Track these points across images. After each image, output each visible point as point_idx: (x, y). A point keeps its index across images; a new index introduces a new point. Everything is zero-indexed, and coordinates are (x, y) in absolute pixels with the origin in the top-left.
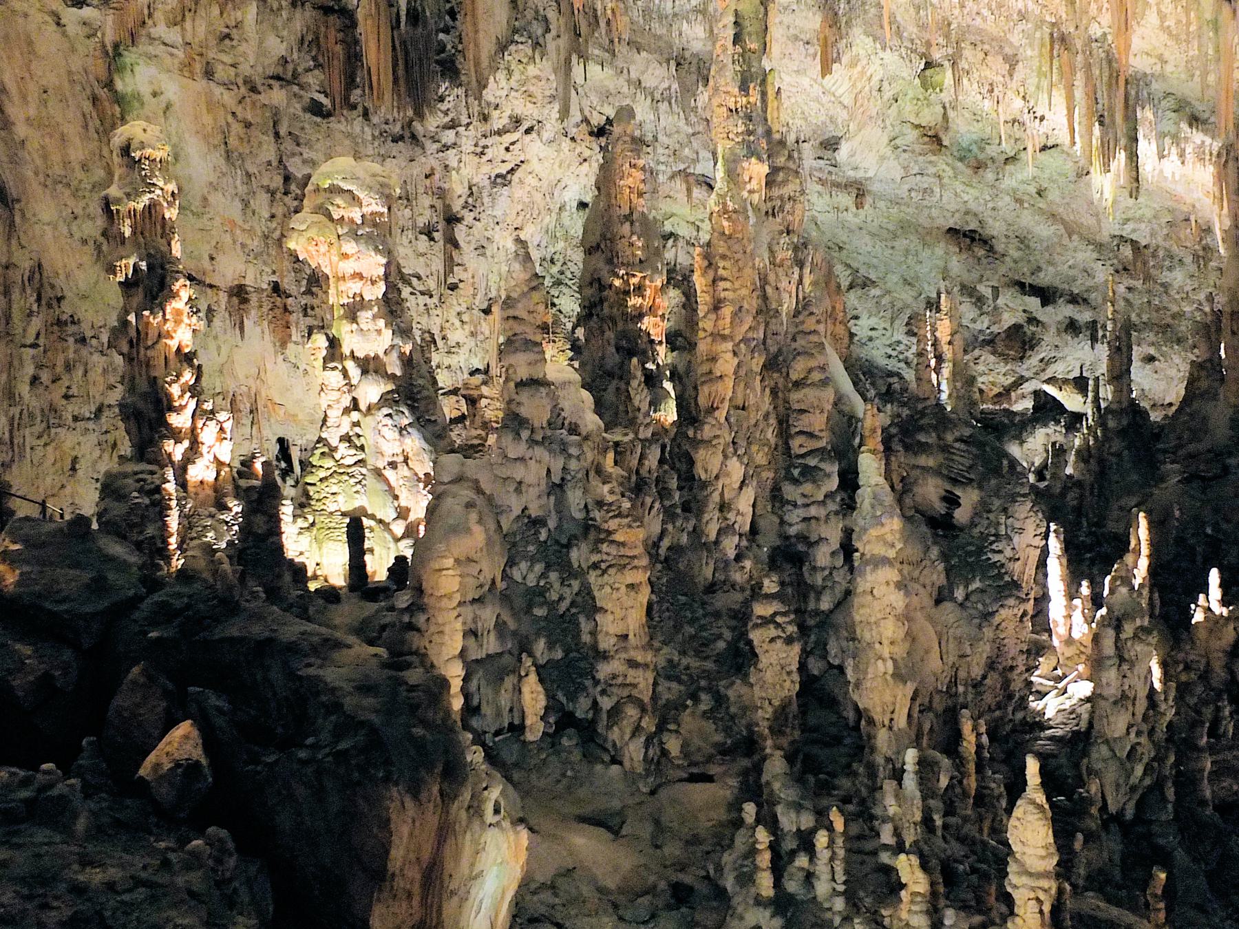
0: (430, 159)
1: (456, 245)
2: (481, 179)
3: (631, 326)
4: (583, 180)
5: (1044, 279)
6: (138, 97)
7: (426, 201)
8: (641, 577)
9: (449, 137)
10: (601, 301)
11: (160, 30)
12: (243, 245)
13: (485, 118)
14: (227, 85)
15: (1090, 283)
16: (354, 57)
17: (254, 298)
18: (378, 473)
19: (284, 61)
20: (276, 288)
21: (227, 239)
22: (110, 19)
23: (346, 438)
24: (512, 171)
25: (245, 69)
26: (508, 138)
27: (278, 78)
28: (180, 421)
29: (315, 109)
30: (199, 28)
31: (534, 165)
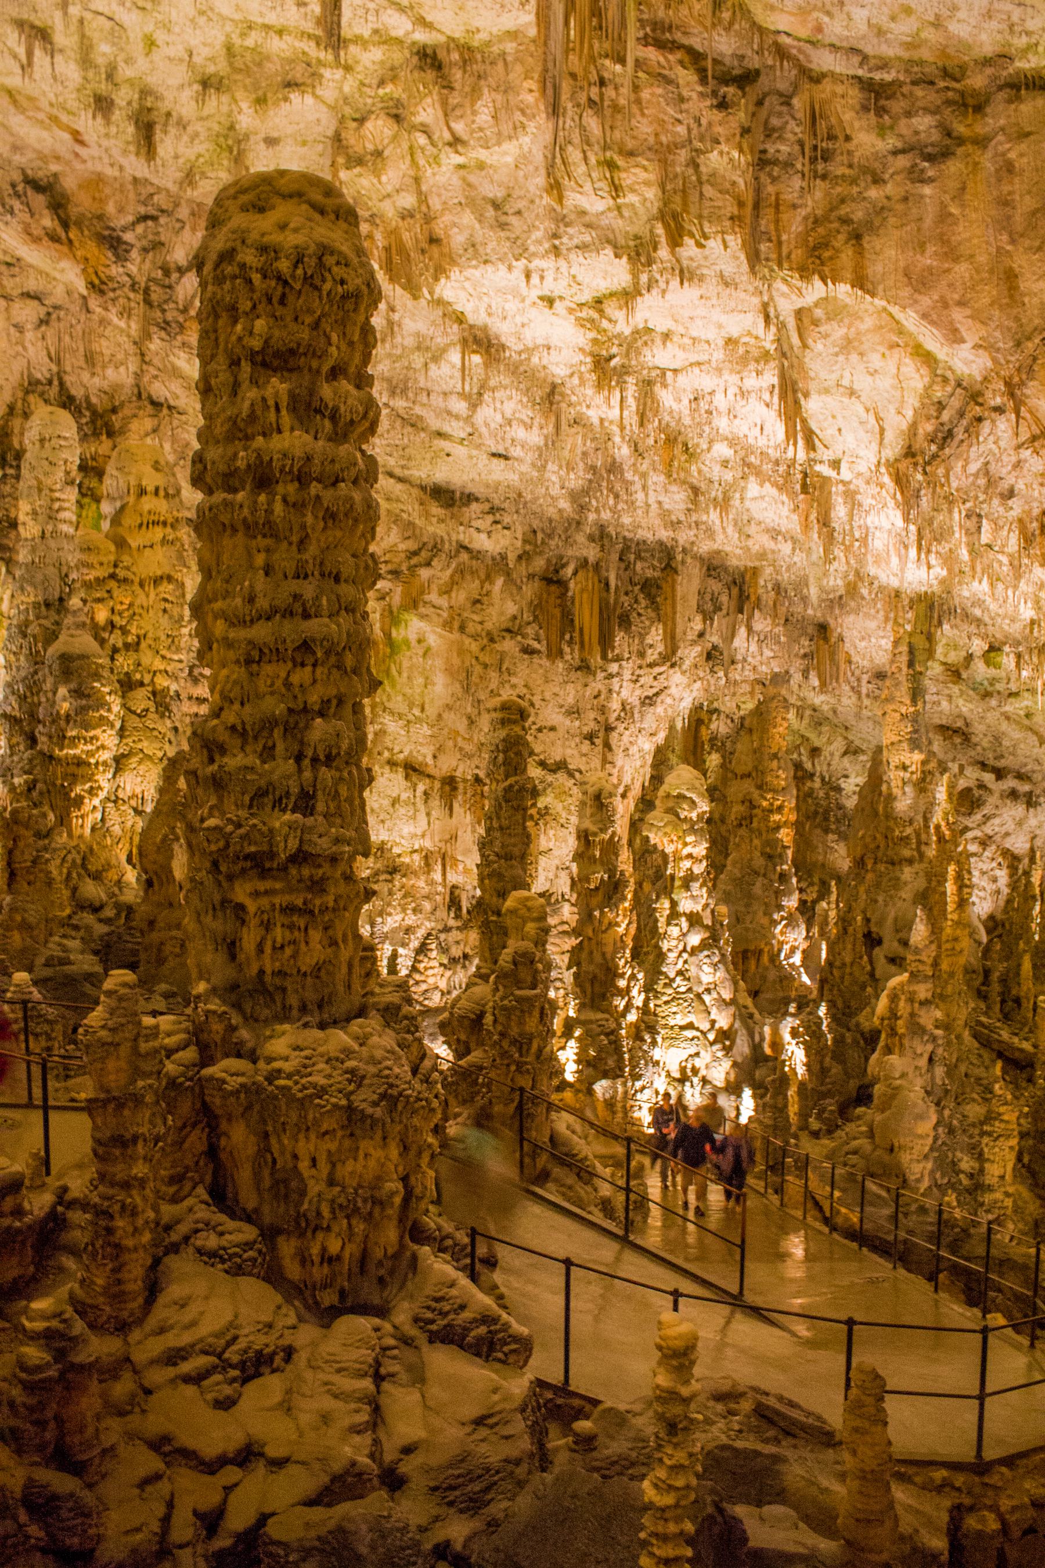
0: (598, 684)
1: (610, 749)
2: (634, 700)
3: (771, 836)
4: (695, 694)
5: (1001, 764)
6: (407, 642)
7: (592, 715)
8: (1014, 1142)
9: (614, 668)
10: (751, 817)
11: (433, 597)
12: (461, 749)
13: (642, 654)
14: (475, 637)
15: (1037, 768)
16: (568, 620)
17: (461, 786)
18: (699, 996)
19: (515, 618)
20: (477, 780)
21: (451, 743)
22: (399, 589)
23: (680, 973)
24: (657, 694)
25: (489, 626)
26: (657, 670)
27: (508, 630)
28: (622, 983)
29: (528, 651)
30: (460, 597)
31: (673, 690)
